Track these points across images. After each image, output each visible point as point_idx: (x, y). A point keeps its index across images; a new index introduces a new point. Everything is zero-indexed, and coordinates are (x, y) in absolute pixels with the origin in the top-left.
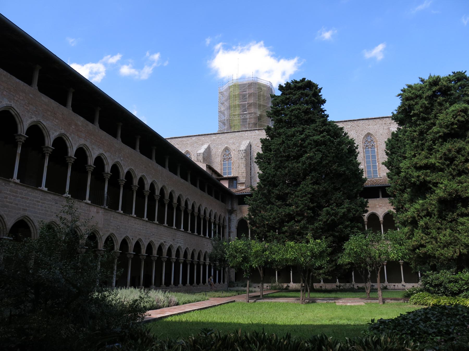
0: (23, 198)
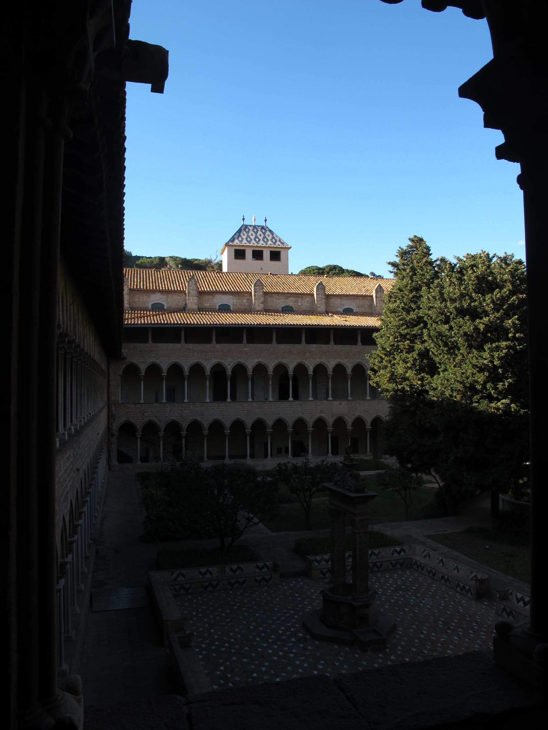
0: (276, 408)
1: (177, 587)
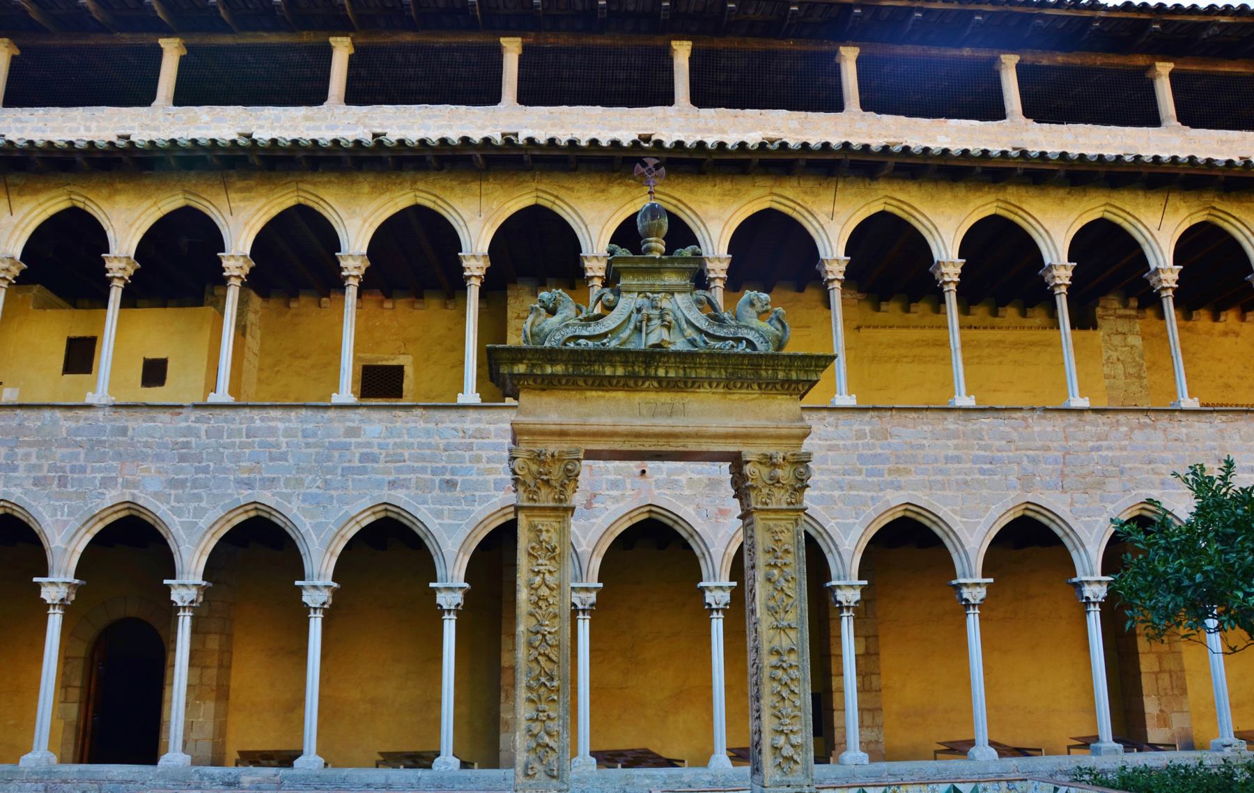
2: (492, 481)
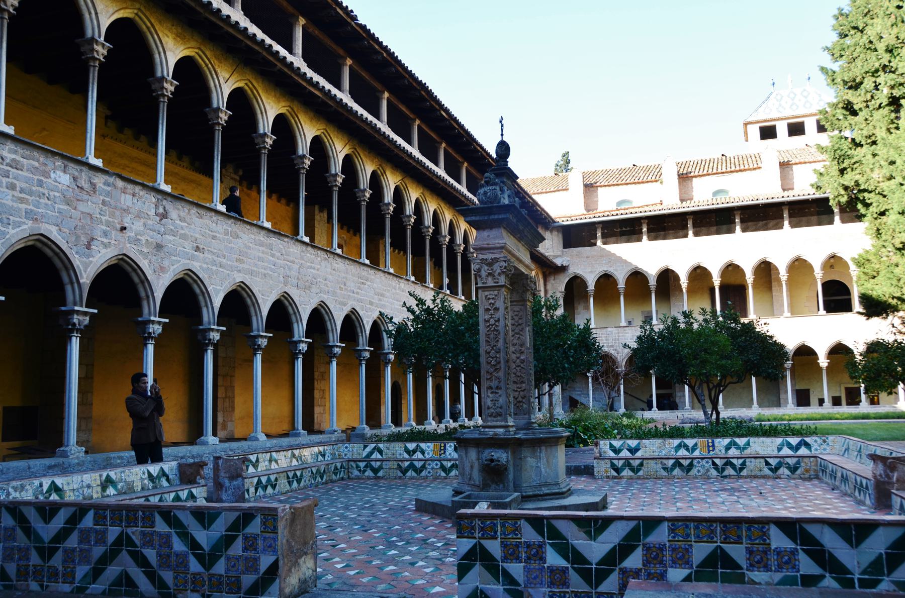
1: (362, 465)
2: (24, 210)
